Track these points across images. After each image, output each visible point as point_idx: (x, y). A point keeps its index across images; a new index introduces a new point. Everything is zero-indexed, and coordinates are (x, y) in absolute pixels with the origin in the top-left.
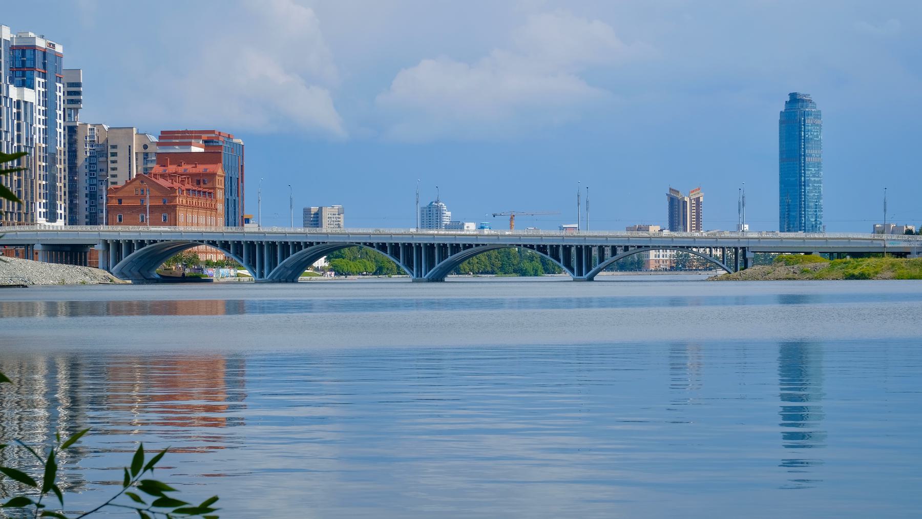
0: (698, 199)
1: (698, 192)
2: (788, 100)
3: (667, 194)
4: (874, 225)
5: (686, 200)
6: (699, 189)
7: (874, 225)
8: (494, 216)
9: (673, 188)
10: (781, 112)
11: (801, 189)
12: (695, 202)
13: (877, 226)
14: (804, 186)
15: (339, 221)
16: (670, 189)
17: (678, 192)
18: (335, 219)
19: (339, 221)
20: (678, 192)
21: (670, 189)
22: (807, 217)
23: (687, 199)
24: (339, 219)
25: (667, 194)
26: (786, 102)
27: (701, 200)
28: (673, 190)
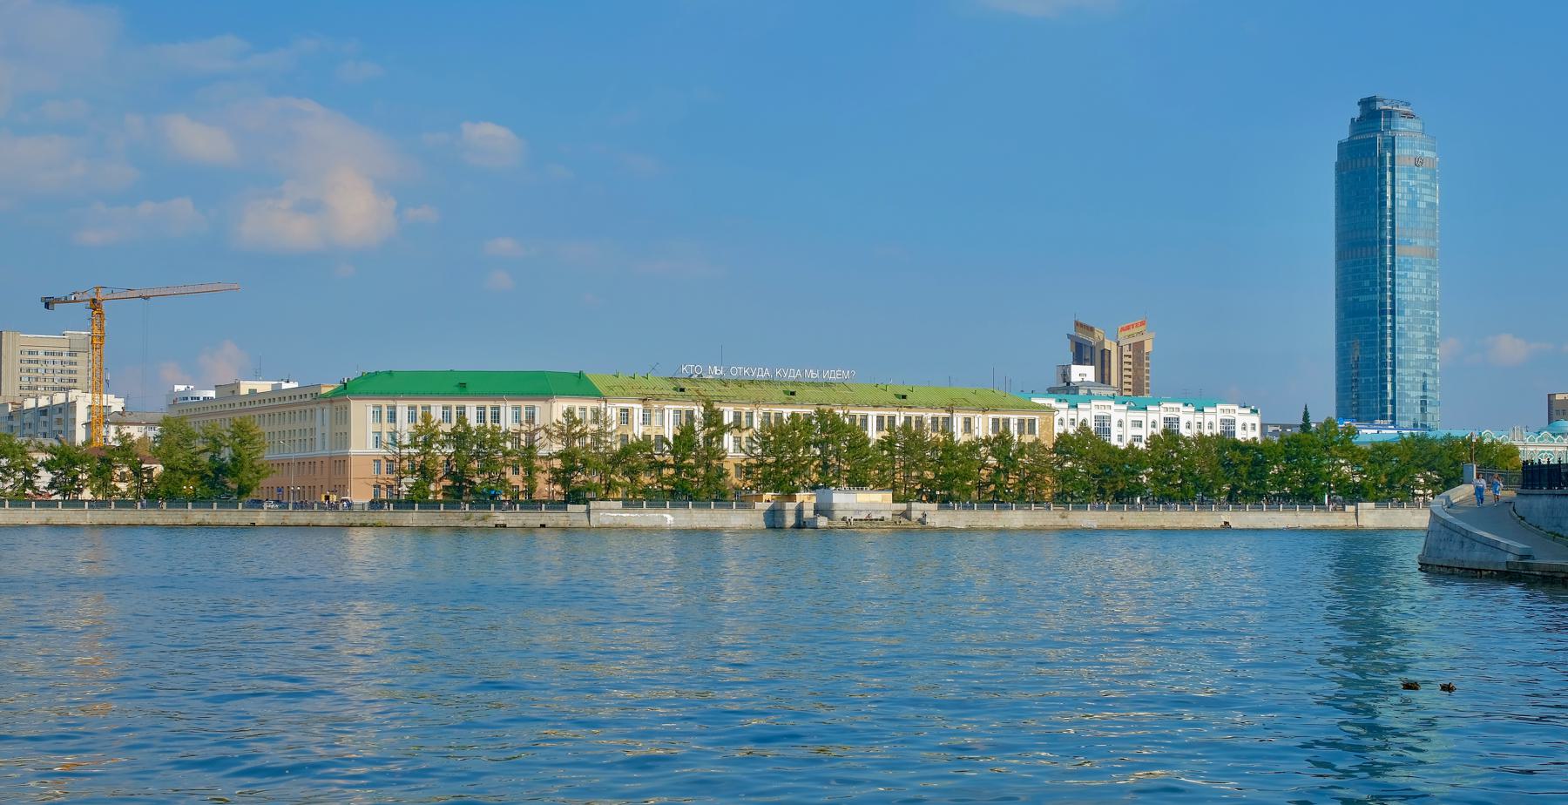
0: (1139, 346)
1: (1141, 329)
2: (1356, 113)
3: (1069, 336)
4: (1549, 395)
5: (1107, 347)
6: (1143, 324)
7: (1549, 395)
8: (47, 306)
9: (1081, 321)
10: (1340, 145)
11: (1384, 320)
12: (1131, 353)
13: (1558, 397)
14: (1393, 312)
15: (70, 372)
16: (1077, 324)
17: (1092, 329)
18: (58, 367)
19: (70, 372)
20: (1092, 329)
21: (1077, 324)
22: (1397, 387)
23: (1109, 345)
24: (73, 367)
25: (1069, 336)
26: (1353, 119)
27: (1148, 347)
28: (1082, 325)
